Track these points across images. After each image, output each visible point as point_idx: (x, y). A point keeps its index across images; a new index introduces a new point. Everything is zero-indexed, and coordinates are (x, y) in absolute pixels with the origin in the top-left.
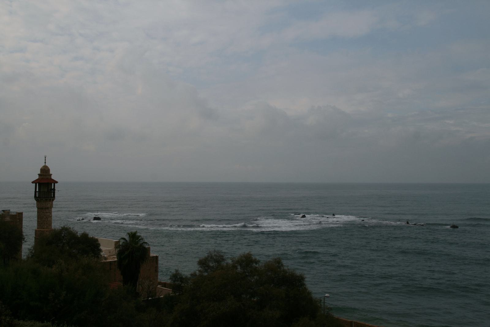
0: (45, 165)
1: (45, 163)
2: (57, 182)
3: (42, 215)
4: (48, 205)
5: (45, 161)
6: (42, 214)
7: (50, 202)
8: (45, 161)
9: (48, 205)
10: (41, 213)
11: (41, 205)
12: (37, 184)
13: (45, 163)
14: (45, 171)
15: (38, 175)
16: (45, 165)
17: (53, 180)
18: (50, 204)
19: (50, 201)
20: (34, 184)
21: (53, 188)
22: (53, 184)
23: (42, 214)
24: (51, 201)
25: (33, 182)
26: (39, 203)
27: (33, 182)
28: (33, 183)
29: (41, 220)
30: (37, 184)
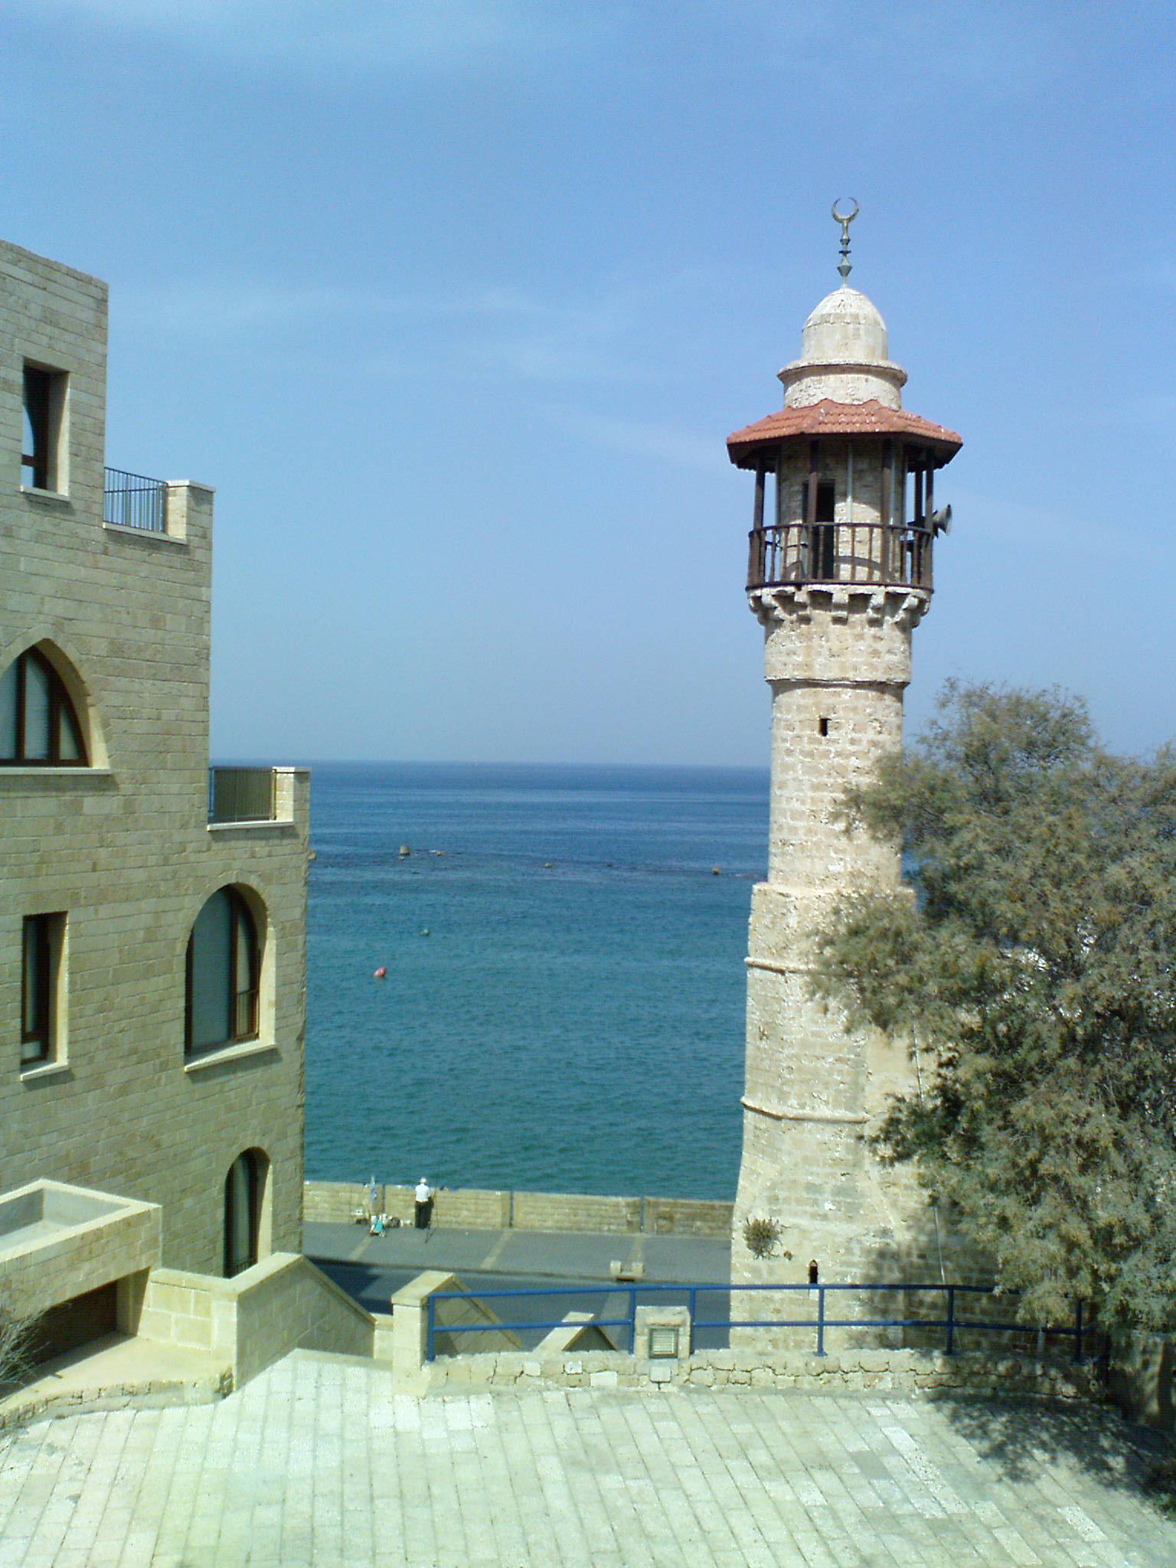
11: (876, 653)
26: (860, 637)
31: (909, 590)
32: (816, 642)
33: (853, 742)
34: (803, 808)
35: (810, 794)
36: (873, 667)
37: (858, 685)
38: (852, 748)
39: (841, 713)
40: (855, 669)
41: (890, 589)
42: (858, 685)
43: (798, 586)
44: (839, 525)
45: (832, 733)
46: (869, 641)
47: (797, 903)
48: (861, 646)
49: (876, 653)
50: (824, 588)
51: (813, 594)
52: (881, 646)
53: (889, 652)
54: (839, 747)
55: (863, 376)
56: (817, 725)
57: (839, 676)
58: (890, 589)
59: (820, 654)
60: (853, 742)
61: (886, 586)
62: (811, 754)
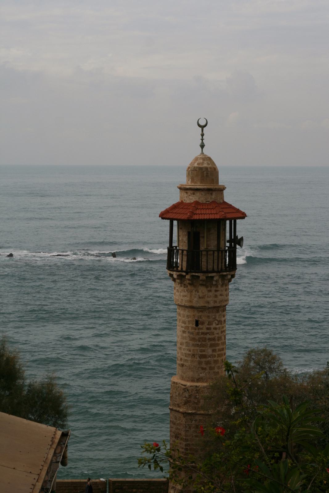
0: (202, 153)
1: (202, 146)
2: (243, 216)
3: (218, 331)
5: (202, 140)
6: (215, 329)
8: (202, 140)
10: (212, 327)
12: (175, 223)
13: (202, 146)
14: (205, 174)
15: (179, 190)
16: (202, 153)
17: (230, 206)
20: (168, 222)
22: (228, 222)
23: (215, 329)
25: (163, 216)
26: (210, 291)
27: (163, 216)
28: (163, 218)
29: (214, 351)
30: (175, 223)
32: (194, 293)
33: (208, 329)
34: (190, 353)
35: (193, 348)
38: (209, 331)
41: (221, 273)
43: (187, 273)
44: (202, 251)
45: (200, 326)
47: (189, 388)
48: (211, 294)
50: (197, 274)
51: (192, 276)
53: (221, 295)
54: (203, 331)
56: (194, 323)
59: (195, 297)
60: (208, 329)
62: (192, 333)
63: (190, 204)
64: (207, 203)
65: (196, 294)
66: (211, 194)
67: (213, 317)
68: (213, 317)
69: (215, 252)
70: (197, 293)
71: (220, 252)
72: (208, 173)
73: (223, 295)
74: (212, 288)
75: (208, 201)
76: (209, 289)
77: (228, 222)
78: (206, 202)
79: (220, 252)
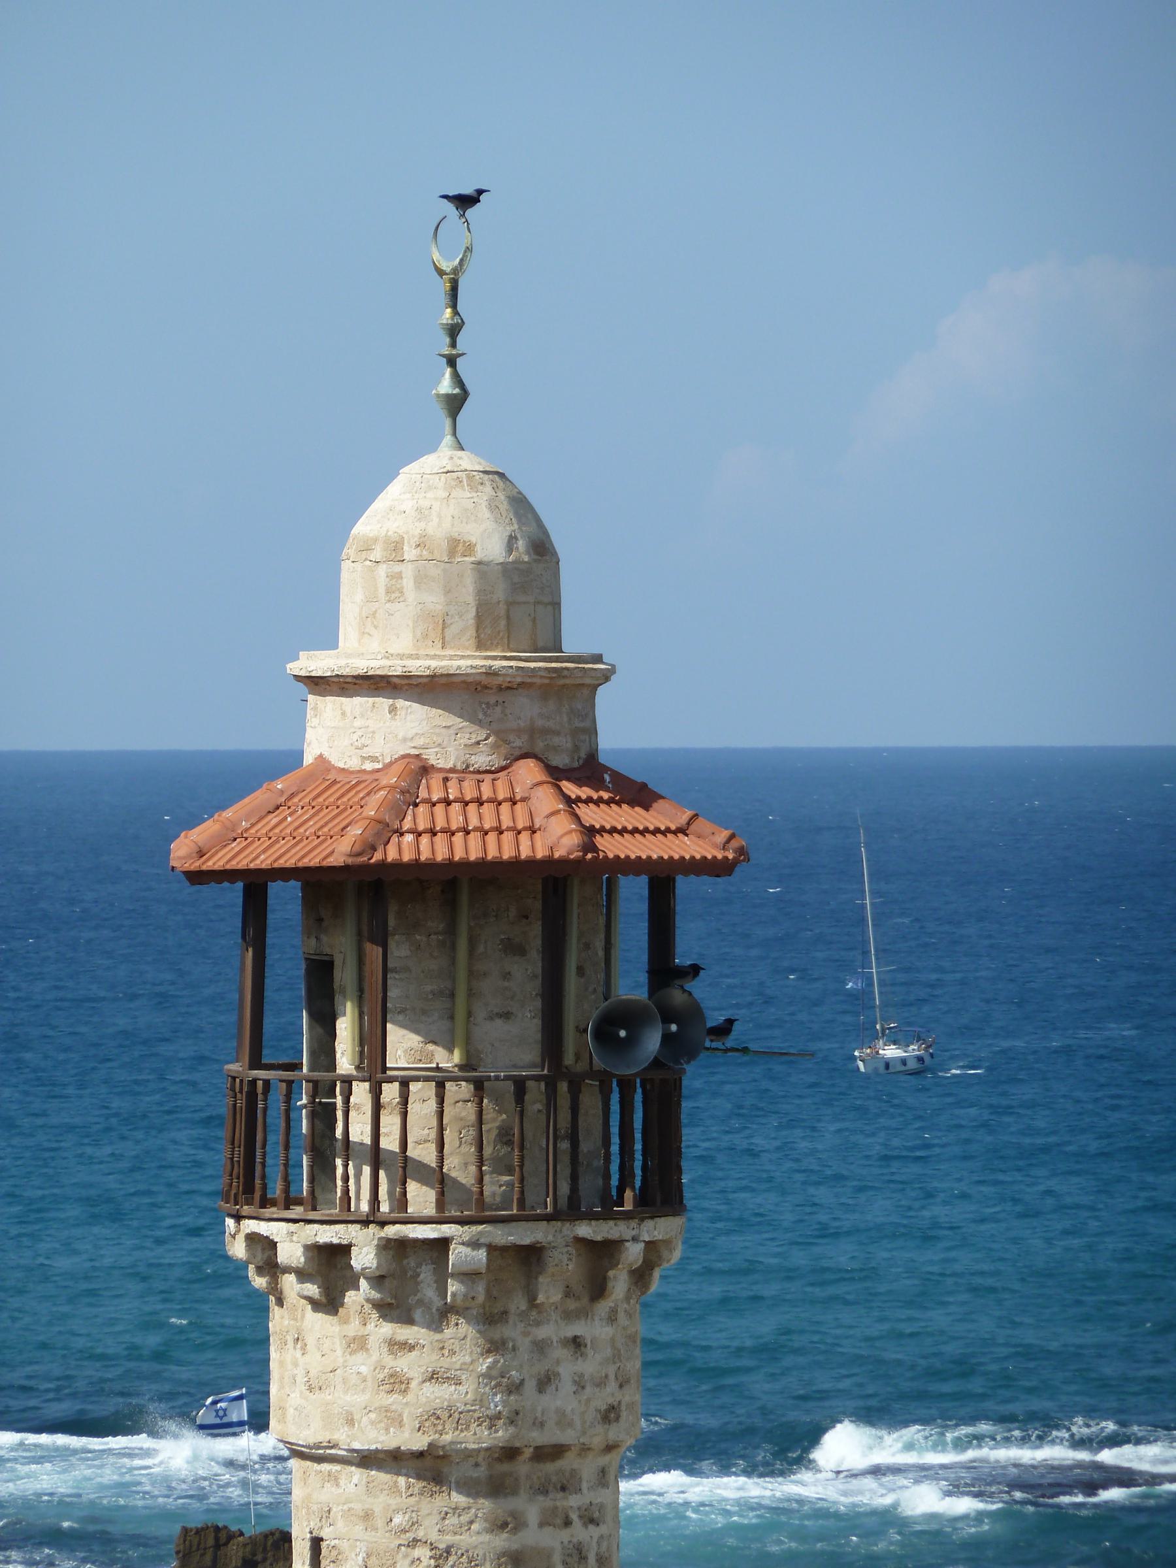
4: (545, 1382)
7: (595, 1330)
9: (562, 1398)
11: (397, 1383)
18: (589, 1366)
19: (598, 1290)
21: (631, 985)
24: (619, 1283)
26: (358, 1344)
31: (447, 1230)
36: (393, 1419)
37: (367, 1460)
39: (340, 1524)
40: (350, 1422)
41: (392, 1231)
42: (367, 1460)
46: (377, 1352)
48: (363, 1364)
49: (397, 1383)
52: (405, 1364)
53: (432, 1377)
55: (384, 703)
57: (322, 1437)
58: (392, 1231)
61: (382, 1224)
63: (361, 782)
64: (369, 766)
65: (296, 1365)
66: (393, 710)
67: (398, 1520)
68: (398, 1520)
69: (414, 1087)
70: (298, 1354)
71: (390, 1092)
72: (399, 576)
73: (459, 1383)
74: (371, 1327)
75: (374, 759)
76: (354, 1328)
77: (633, 895)
78: (364, 758)
79: (390, 1092)
